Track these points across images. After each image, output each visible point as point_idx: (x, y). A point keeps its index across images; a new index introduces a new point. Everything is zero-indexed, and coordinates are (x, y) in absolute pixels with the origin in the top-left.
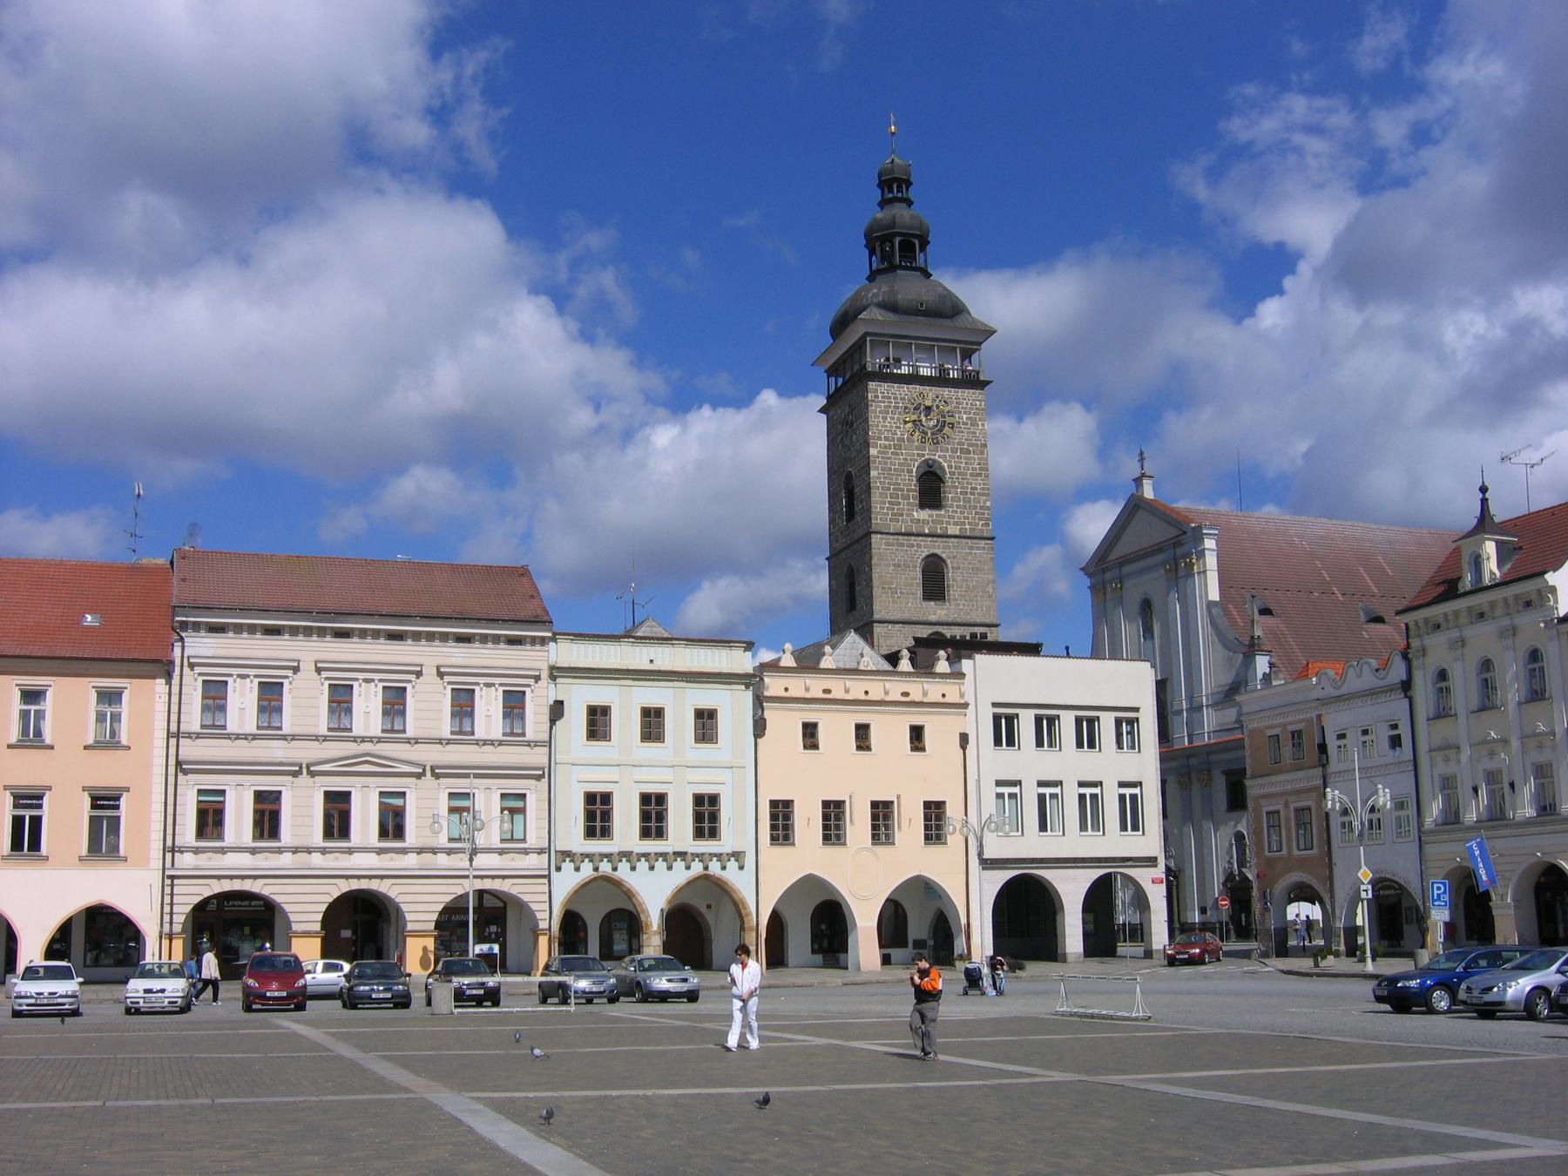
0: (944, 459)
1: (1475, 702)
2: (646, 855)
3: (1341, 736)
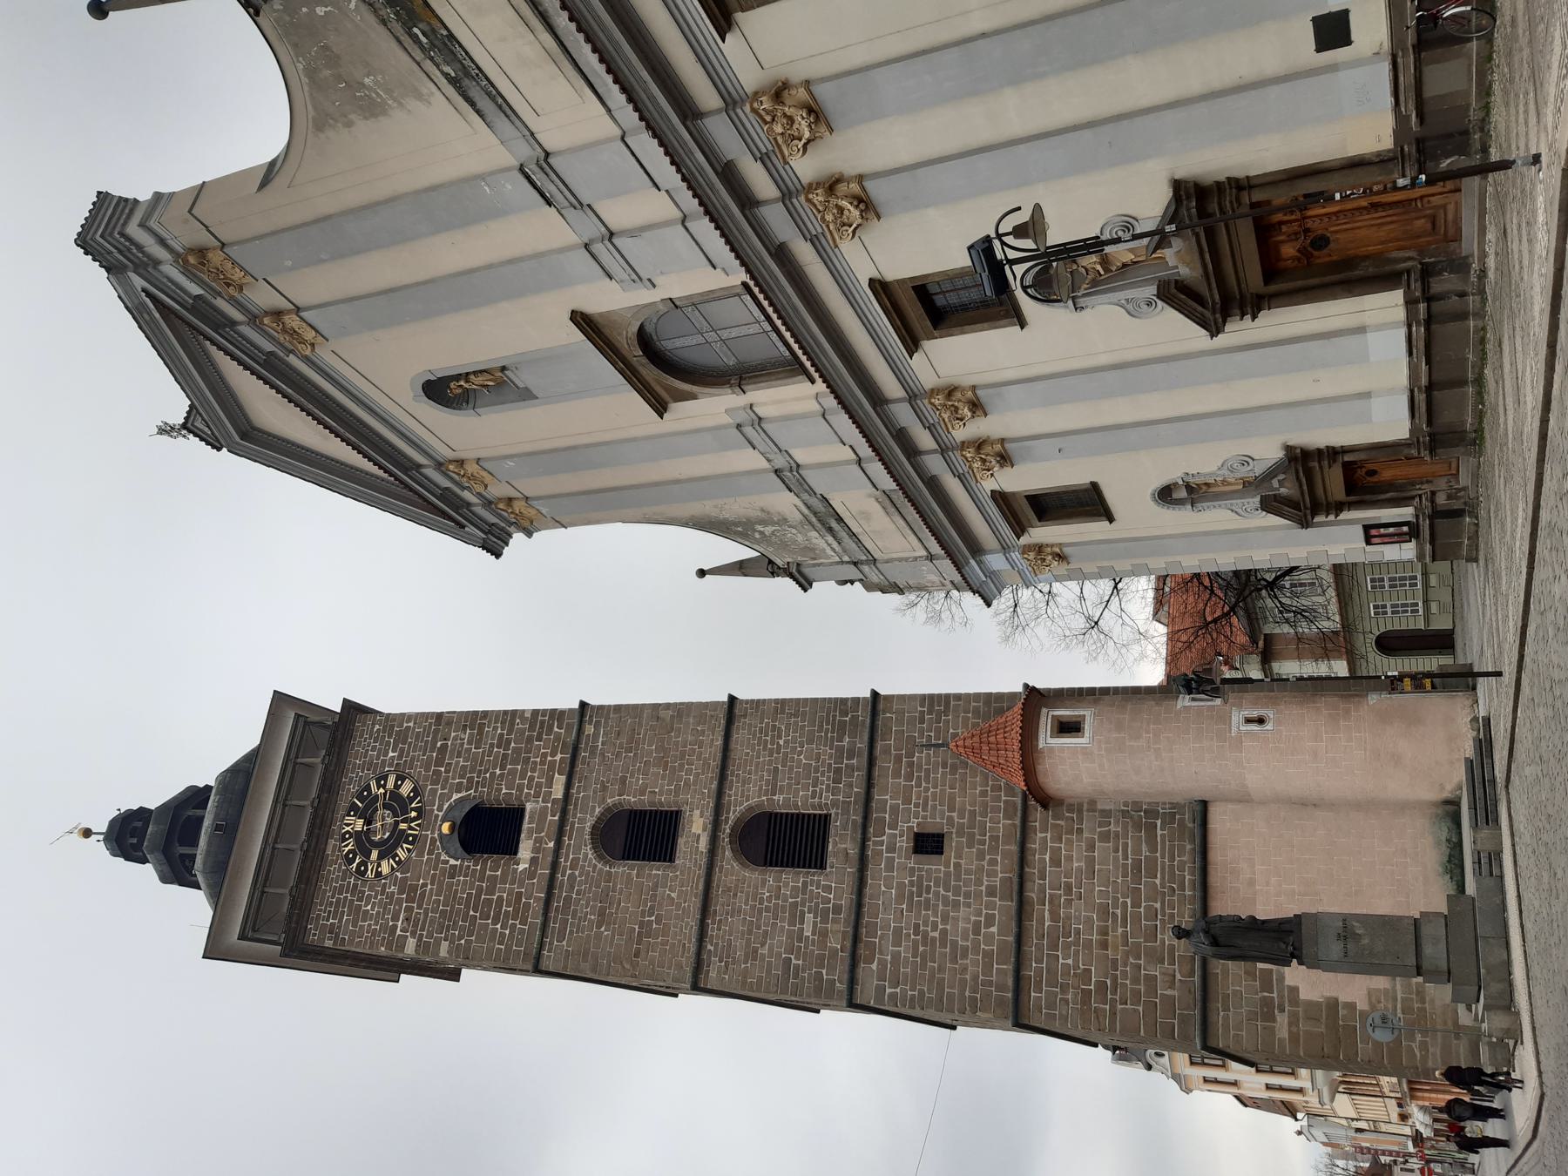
0: (446, 803)
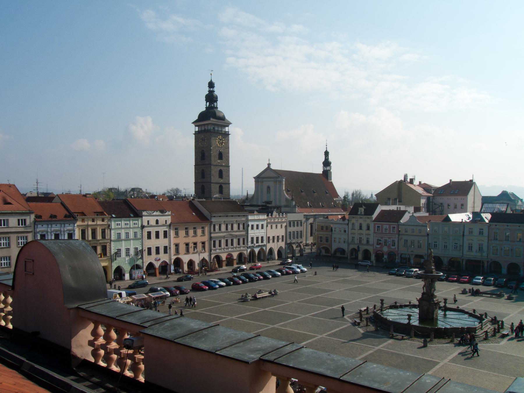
1: (359, 228)
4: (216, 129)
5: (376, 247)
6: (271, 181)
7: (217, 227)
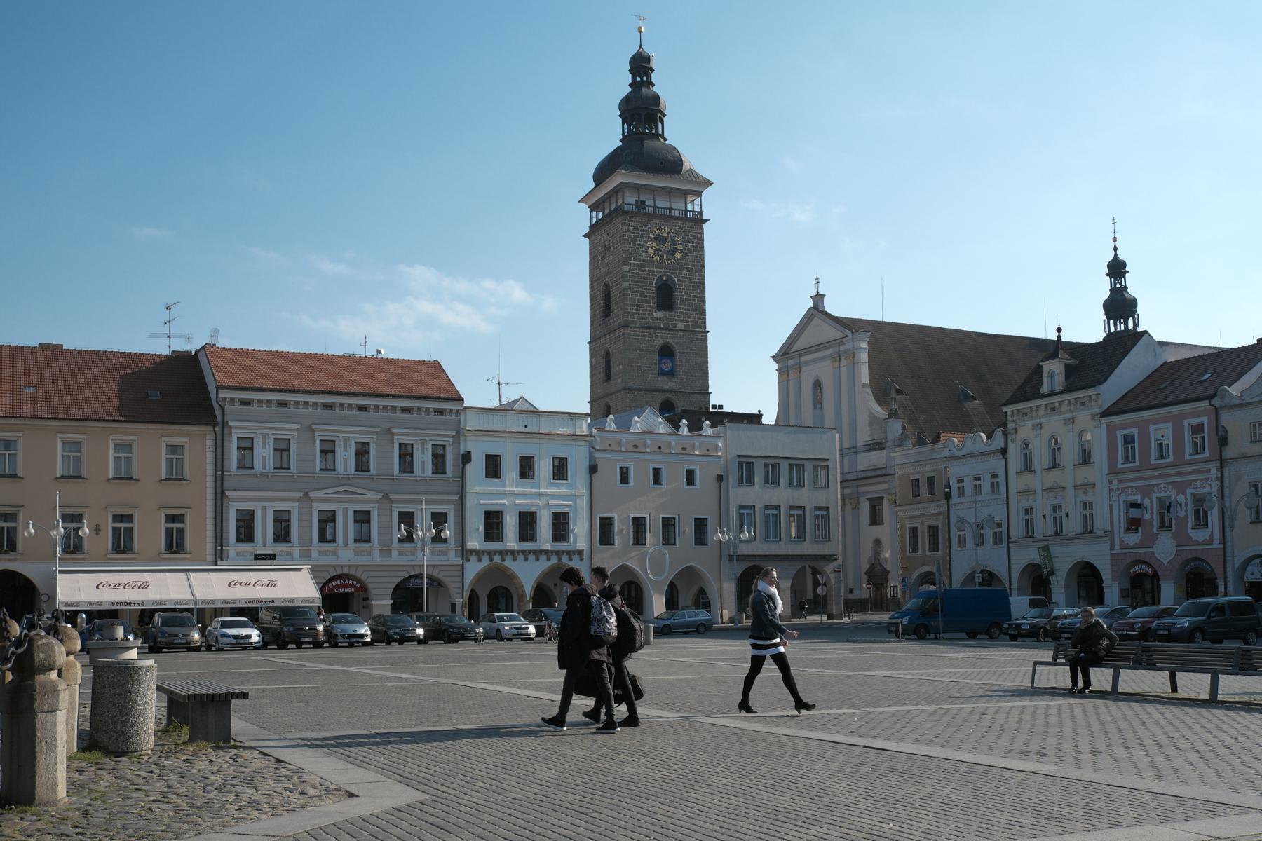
2: (523, 552)
3: (960, 481)
4: (649, 203)
5: (1124, 546)
6: (824, 358)
7: (264, 455)
